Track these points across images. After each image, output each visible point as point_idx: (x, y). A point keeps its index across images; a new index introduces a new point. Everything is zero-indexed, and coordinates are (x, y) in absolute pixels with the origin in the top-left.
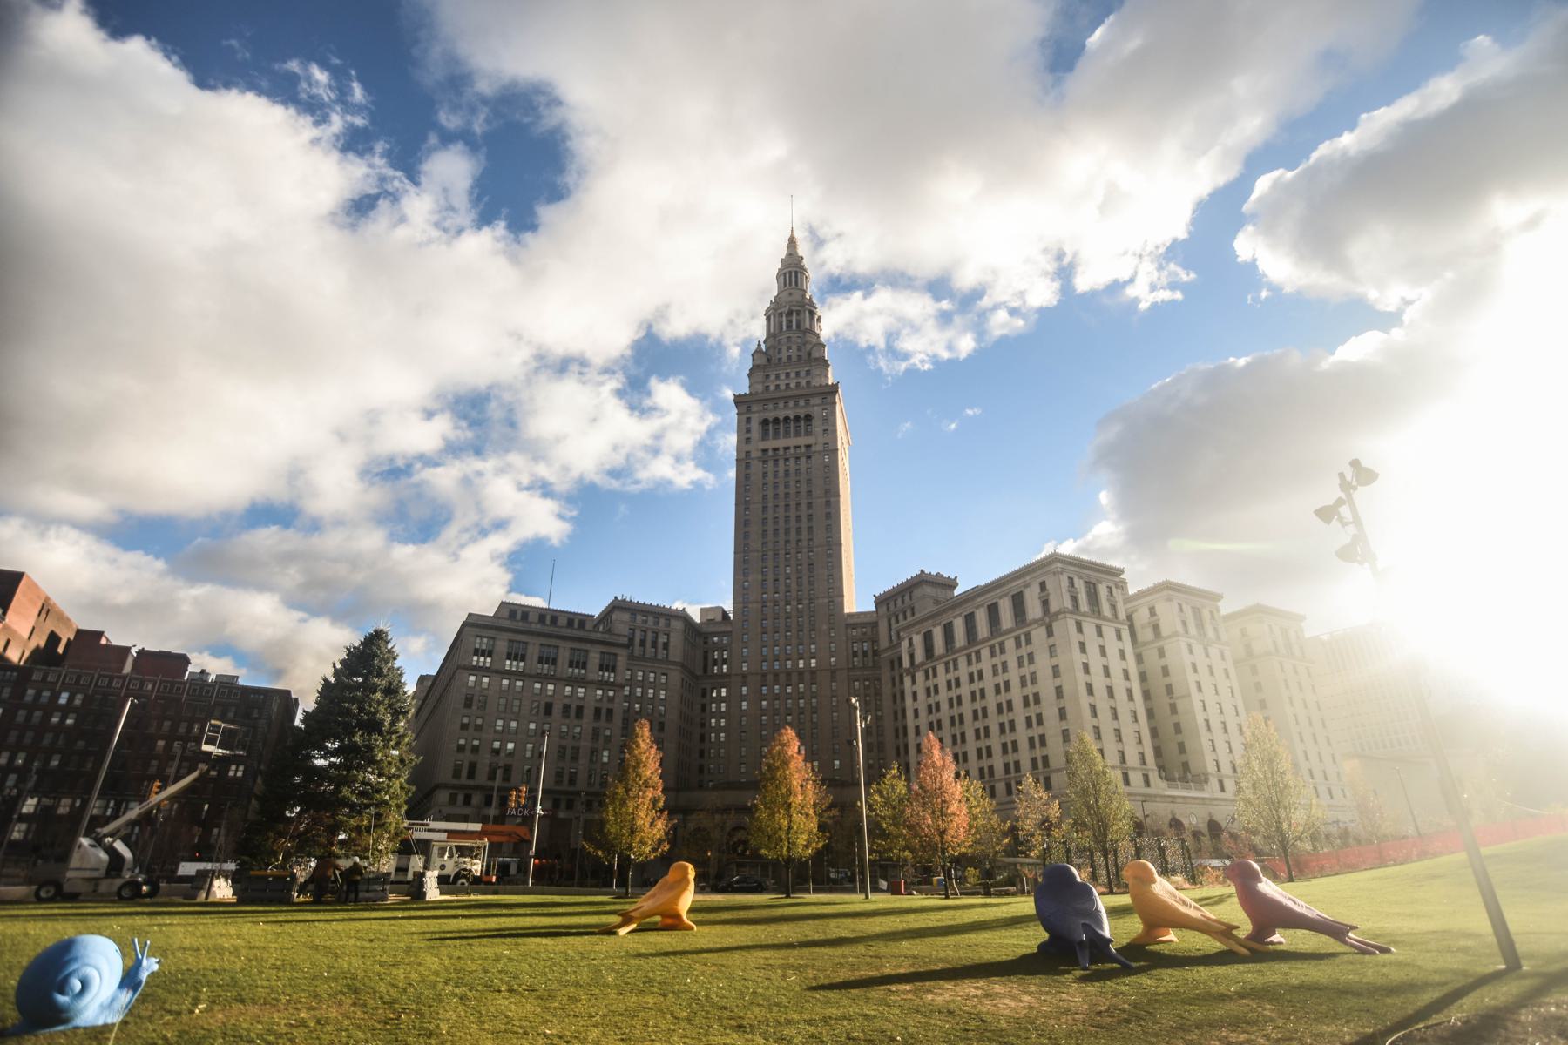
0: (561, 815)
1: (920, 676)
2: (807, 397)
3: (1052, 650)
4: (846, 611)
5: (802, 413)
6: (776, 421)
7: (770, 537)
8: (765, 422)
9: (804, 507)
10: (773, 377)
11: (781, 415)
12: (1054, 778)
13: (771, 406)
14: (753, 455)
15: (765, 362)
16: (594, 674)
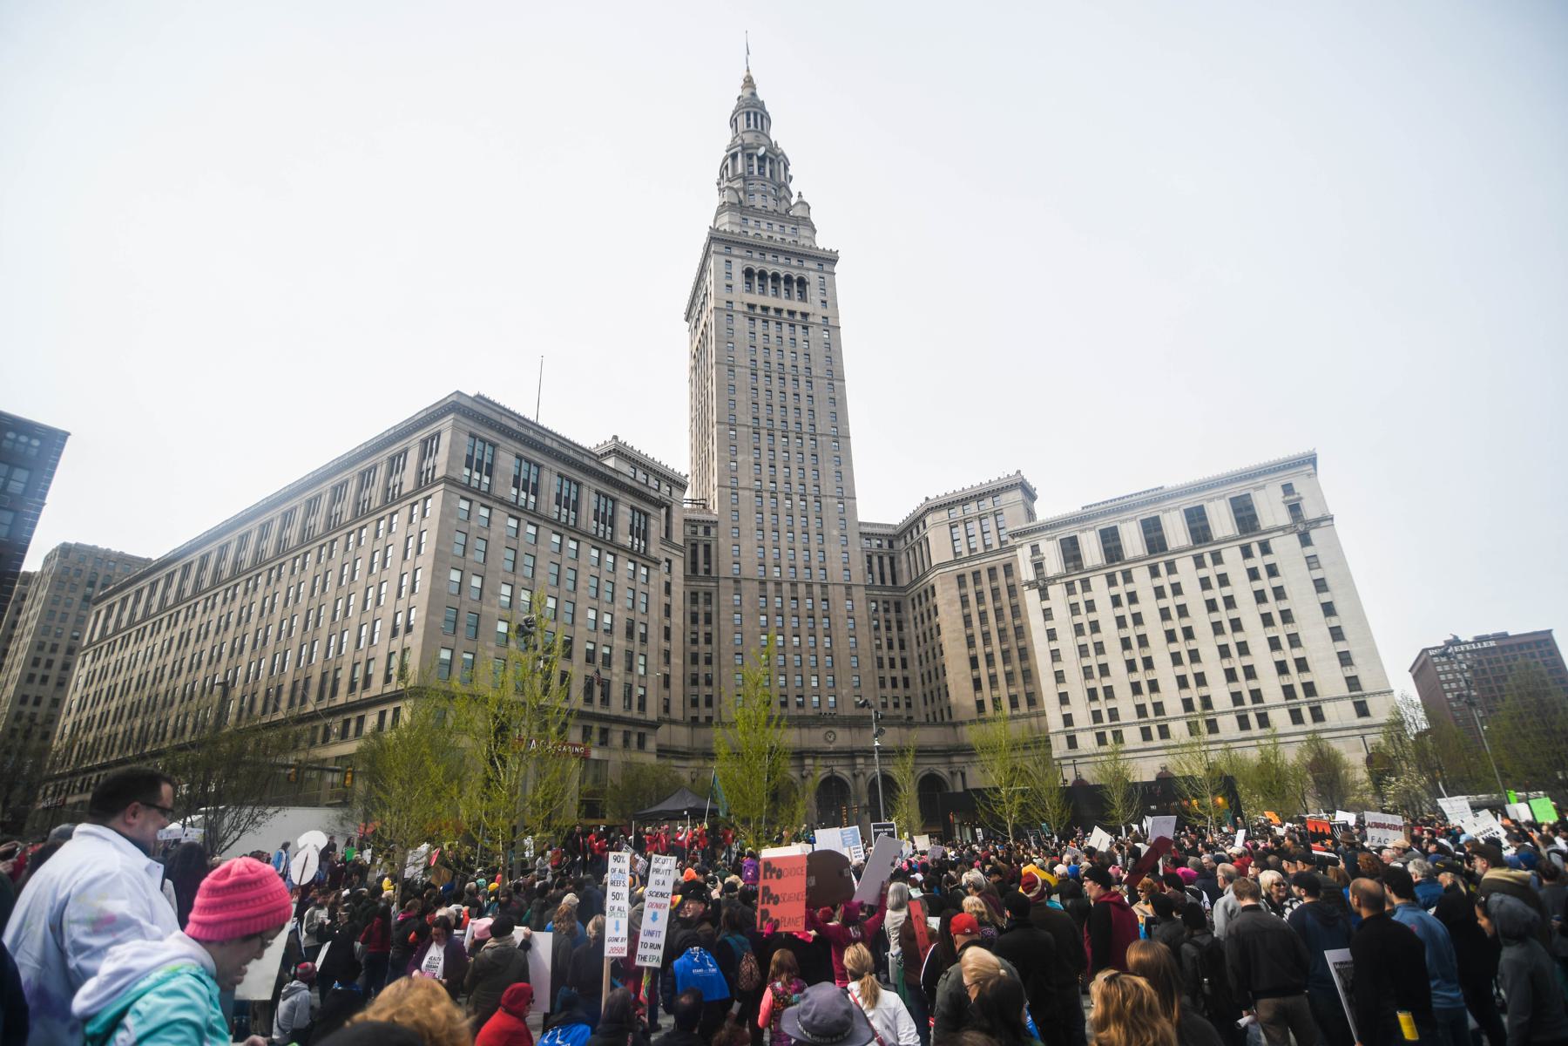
0: (595, 754)
1: (1056, 591)
2: (802, 256)
3: (1312, 562)
4: (861, 518)
5: (795, 274)
6: (762, 275)
7: (763, 412)
8: (749, 273)
9: (803, 384)
10: (751, 223)
11: (770, 269)
12: (1327, 709)
13: (756, 255)
14: (737, 307)
15: (736, 207)
16: (625, 539)
